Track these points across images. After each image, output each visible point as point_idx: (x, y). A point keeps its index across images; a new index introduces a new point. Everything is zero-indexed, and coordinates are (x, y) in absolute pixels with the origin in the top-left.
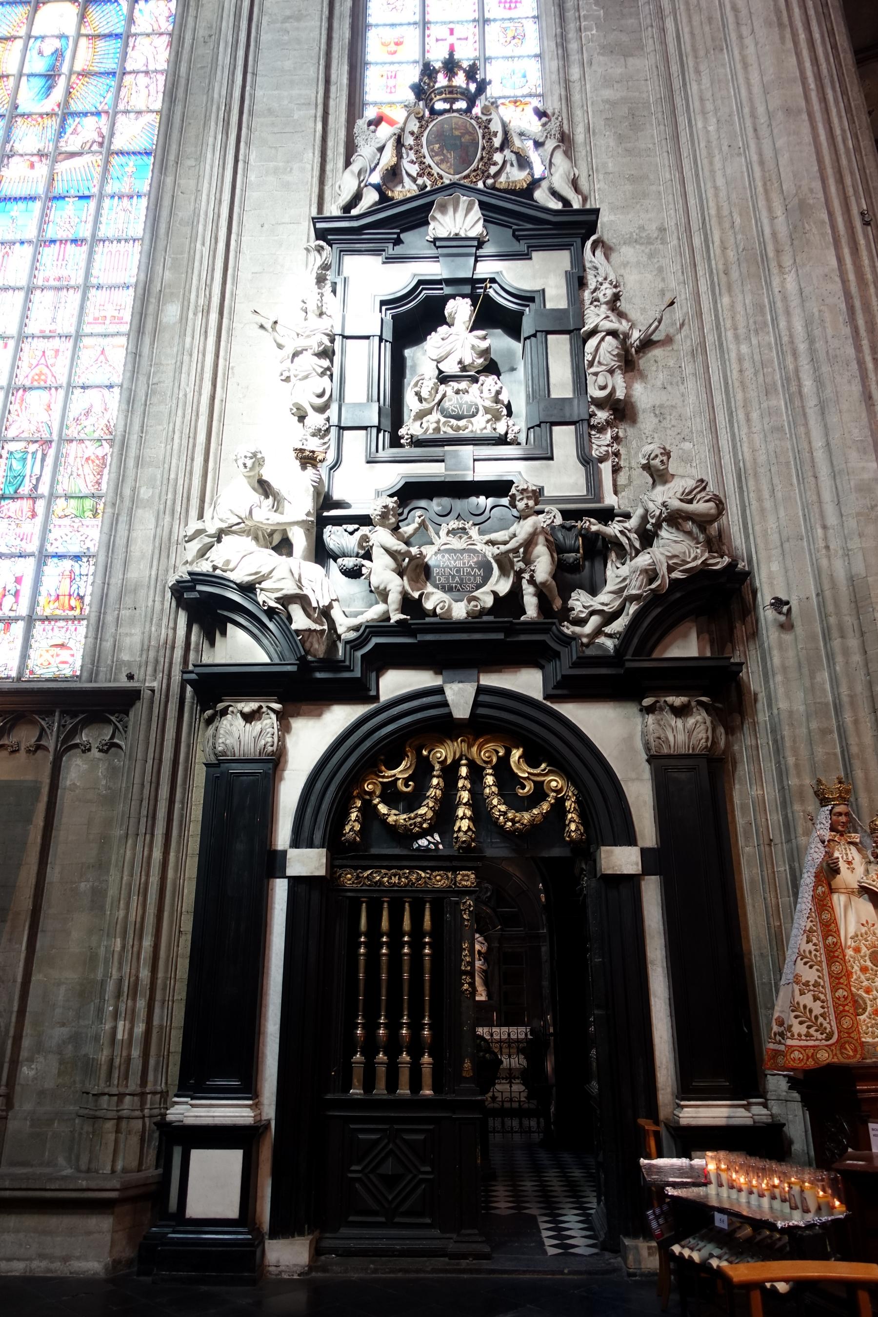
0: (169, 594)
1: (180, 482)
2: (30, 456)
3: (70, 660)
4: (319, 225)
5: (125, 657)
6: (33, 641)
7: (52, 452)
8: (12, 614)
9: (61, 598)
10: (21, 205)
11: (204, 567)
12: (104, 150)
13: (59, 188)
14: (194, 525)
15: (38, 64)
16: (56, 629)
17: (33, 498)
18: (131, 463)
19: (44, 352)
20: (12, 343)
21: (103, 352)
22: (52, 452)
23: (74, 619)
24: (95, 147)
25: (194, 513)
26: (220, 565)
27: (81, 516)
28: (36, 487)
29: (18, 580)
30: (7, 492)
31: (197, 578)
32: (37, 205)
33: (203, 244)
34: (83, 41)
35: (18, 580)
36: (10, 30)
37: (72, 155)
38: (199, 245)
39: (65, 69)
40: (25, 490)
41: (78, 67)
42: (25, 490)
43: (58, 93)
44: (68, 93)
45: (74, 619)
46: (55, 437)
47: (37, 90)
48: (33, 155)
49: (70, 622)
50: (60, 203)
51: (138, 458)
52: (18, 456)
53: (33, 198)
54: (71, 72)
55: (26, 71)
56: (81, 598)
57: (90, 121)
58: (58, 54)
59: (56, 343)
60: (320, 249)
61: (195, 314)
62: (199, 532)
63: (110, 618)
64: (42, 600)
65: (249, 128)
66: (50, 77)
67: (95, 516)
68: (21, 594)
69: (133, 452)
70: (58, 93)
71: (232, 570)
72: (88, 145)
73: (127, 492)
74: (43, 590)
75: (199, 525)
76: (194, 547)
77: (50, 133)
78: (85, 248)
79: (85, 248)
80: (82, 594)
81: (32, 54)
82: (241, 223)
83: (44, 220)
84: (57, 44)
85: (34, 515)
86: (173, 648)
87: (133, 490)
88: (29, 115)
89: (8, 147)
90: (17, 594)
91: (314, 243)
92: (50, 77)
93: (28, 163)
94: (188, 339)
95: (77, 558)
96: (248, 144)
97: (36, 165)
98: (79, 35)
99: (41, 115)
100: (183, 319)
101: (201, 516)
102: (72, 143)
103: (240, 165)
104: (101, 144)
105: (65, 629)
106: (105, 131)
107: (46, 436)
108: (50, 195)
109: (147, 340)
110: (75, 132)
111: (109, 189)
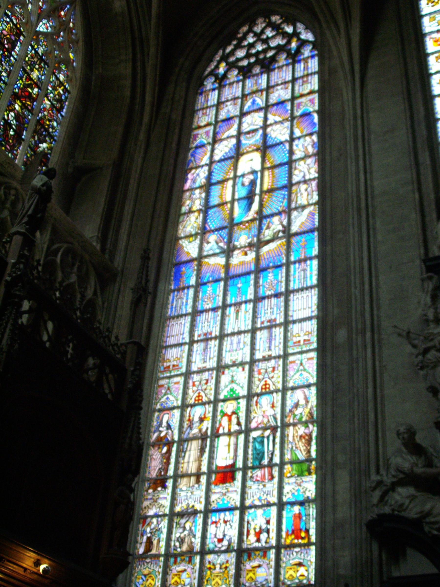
0: (364, 529)
1: (362, 450)
2: (266, 440)
3: (306, 574)
4: (428, 264)
5: (342, 572)
6: (282, 562)
7: (278, 434)
8: (267, 546)
9: (295, 532)
10: (243, 279)
11: (387, 510)
12: (286, 234)
13: (263, 264)
14: (374, 478)
15: (241, 192)
16: (295, 553)
17: (271, 466)
18: (329, 438)
19: (266, 370)
20: (247, 367)
21: (301, 364)
22: (278, 434)
23: (304, 545)
24: (281, 234)
25: (373, 470)
26: (396, 509)
27: (301, 474)
28: (271, 459)
29: (268, 522)
30: (255, 464)
31: (382, 517)
32: (252, 276)
33: (355, 288)
34: (266, 173)
35: (268, 522)
36: (225, 176)
37: (268, 242)
38: (353, 290)
39: (258, 191)
40: (265, 461)
41: (265, 188)
42: (265, 461)
43: (255, 206)
44: (261, 205)
45: (304, 545)
46: (279, 424)
47: (243, 207)
48: (245, 247)
49: (303, 548)
50: (265, 273)
51: (333, 435)
52: (259, 440)
53: (248, 273)
54: (262, 191)
55: (236, 197)
56: (307, 531)
57: (276, 219)
58: (253, 183)
59: (272, 363)
60: (430, 278)
61: (357, 335)
62: (380, 483)
63: (329, 545)
64: (284, 534)
65: (373, 207)
66: (250, 198)
67: (310, 473)
68: (271, 531)
69: (329, 431)
70: (255, 206)
71: (405, 510)
72: (277, 234)
73: (329, 458)
74: (284, 527)
75: (378, 478)
76: (377, 494)
77: (255, 231)
78: (282, 299)
79: (282, 299)
80: (308, 528)
81: (239, 186)
82: (377, 270)
83: (256, 286)
84: (251, 177)
85: (272, 478)
86: (372, 564)
87: (333, 457)
88: (241, 223)
89: (231, 245)
90: (268, 531)
91: (425, 275)
92: (250, 198)
93: (244, 252)
94: (355, 353)
95: (301, 504)
96: (374, 218)
97: (249, 252)
98: (263, 169)
99: (248, 222)
100: (350, 339)
101: (378, 472)
102: (267, 234)
103: (371, 232)
104: (284, 232)
105: (300, 553)
106: (285, 222)
107: (273, 423)
108: (259, 270)
109: (329, 354)
110: (268, 228)
111: (293, 259)
